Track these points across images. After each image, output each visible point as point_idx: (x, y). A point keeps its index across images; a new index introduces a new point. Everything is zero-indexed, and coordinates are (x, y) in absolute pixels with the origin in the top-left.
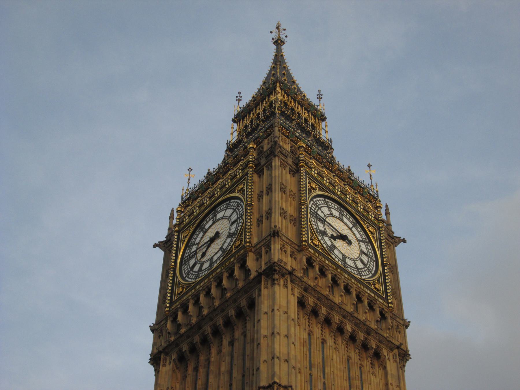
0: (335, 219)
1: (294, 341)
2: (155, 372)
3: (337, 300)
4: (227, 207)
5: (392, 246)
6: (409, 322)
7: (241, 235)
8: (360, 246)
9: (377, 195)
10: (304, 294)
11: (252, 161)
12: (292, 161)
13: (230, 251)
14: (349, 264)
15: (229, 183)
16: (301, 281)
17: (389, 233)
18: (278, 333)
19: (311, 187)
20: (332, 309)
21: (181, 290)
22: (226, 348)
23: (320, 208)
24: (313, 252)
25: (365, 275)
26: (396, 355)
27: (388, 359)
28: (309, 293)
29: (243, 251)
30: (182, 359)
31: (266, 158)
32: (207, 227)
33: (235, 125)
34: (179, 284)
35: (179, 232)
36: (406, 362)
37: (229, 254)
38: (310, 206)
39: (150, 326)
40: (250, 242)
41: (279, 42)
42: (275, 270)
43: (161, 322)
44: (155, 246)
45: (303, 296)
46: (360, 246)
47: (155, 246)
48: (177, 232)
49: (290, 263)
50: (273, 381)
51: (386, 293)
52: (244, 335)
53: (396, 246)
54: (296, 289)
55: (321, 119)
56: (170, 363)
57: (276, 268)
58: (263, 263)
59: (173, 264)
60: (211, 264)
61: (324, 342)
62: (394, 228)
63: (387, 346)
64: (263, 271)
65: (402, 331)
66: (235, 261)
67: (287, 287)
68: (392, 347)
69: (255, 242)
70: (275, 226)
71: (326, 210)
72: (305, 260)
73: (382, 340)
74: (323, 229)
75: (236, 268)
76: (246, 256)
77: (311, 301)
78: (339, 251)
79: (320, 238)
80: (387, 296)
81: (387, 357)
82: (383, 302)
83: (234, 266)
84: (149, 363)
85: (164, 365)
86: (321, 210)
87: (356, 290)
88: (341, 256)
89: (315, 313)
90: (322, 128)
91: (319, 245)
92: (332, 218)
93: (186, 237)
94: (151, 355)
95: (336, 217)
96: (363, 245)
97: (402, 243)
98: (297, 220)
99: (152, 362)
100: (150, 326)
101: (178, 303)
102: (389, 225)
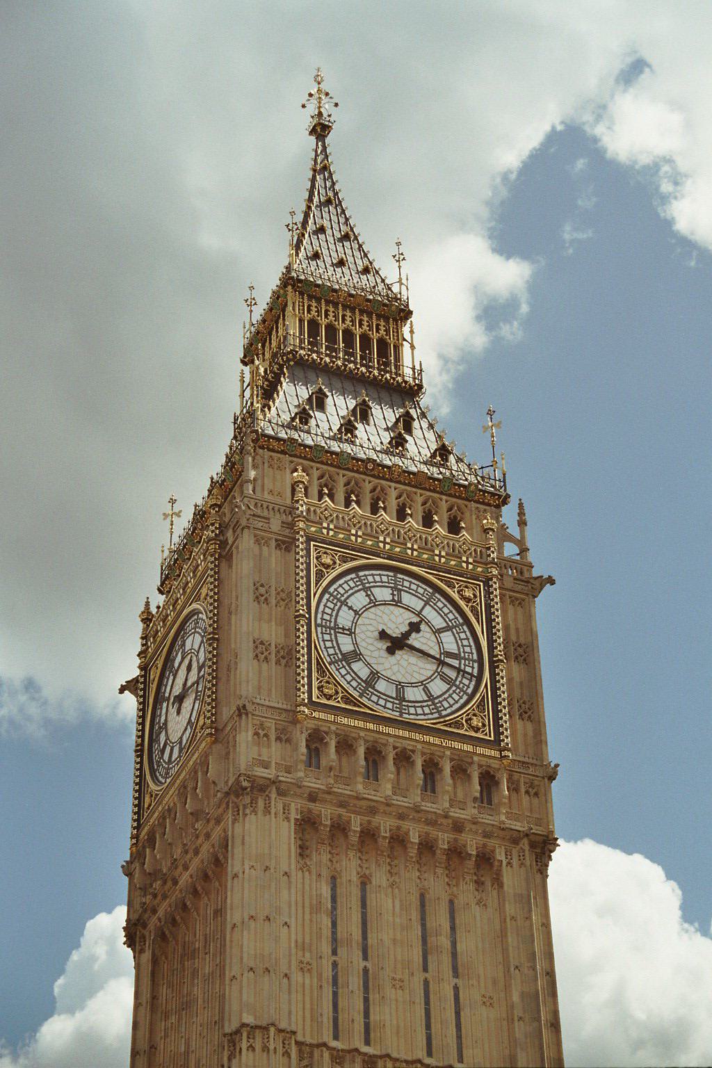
4: (195, 628)
6: (557, 766)
8: (440, 643)
10: (311, 805)
17: (522, 573)
19: (323, 565)
20: (373, 811)
23: (344, 603)
25: (451, 706)
26: (524, 851)
27: (509, 863)
32: (176, 665)
33: (247, 369)
36: (550, 858)
44: (122, 691)
45: (310, 811)
46: (440, 643)
47: (122, 691)
51: (497, 726)
57: (245, 784)
62: (531, 557)
67: (270, 813)
71: (359, 600)
77: (326, 813)
78: (388, 680)
80: (498, 734)
81: (504, 863)
84: (124, 944)
85: (142, 951)
86: (346, 605)
90: (405, 340)
91: (337, 693)
93: (154, 680)
95: (385, 604)
100: (123, 867)
101: (146, 829)
102: (524, 550)
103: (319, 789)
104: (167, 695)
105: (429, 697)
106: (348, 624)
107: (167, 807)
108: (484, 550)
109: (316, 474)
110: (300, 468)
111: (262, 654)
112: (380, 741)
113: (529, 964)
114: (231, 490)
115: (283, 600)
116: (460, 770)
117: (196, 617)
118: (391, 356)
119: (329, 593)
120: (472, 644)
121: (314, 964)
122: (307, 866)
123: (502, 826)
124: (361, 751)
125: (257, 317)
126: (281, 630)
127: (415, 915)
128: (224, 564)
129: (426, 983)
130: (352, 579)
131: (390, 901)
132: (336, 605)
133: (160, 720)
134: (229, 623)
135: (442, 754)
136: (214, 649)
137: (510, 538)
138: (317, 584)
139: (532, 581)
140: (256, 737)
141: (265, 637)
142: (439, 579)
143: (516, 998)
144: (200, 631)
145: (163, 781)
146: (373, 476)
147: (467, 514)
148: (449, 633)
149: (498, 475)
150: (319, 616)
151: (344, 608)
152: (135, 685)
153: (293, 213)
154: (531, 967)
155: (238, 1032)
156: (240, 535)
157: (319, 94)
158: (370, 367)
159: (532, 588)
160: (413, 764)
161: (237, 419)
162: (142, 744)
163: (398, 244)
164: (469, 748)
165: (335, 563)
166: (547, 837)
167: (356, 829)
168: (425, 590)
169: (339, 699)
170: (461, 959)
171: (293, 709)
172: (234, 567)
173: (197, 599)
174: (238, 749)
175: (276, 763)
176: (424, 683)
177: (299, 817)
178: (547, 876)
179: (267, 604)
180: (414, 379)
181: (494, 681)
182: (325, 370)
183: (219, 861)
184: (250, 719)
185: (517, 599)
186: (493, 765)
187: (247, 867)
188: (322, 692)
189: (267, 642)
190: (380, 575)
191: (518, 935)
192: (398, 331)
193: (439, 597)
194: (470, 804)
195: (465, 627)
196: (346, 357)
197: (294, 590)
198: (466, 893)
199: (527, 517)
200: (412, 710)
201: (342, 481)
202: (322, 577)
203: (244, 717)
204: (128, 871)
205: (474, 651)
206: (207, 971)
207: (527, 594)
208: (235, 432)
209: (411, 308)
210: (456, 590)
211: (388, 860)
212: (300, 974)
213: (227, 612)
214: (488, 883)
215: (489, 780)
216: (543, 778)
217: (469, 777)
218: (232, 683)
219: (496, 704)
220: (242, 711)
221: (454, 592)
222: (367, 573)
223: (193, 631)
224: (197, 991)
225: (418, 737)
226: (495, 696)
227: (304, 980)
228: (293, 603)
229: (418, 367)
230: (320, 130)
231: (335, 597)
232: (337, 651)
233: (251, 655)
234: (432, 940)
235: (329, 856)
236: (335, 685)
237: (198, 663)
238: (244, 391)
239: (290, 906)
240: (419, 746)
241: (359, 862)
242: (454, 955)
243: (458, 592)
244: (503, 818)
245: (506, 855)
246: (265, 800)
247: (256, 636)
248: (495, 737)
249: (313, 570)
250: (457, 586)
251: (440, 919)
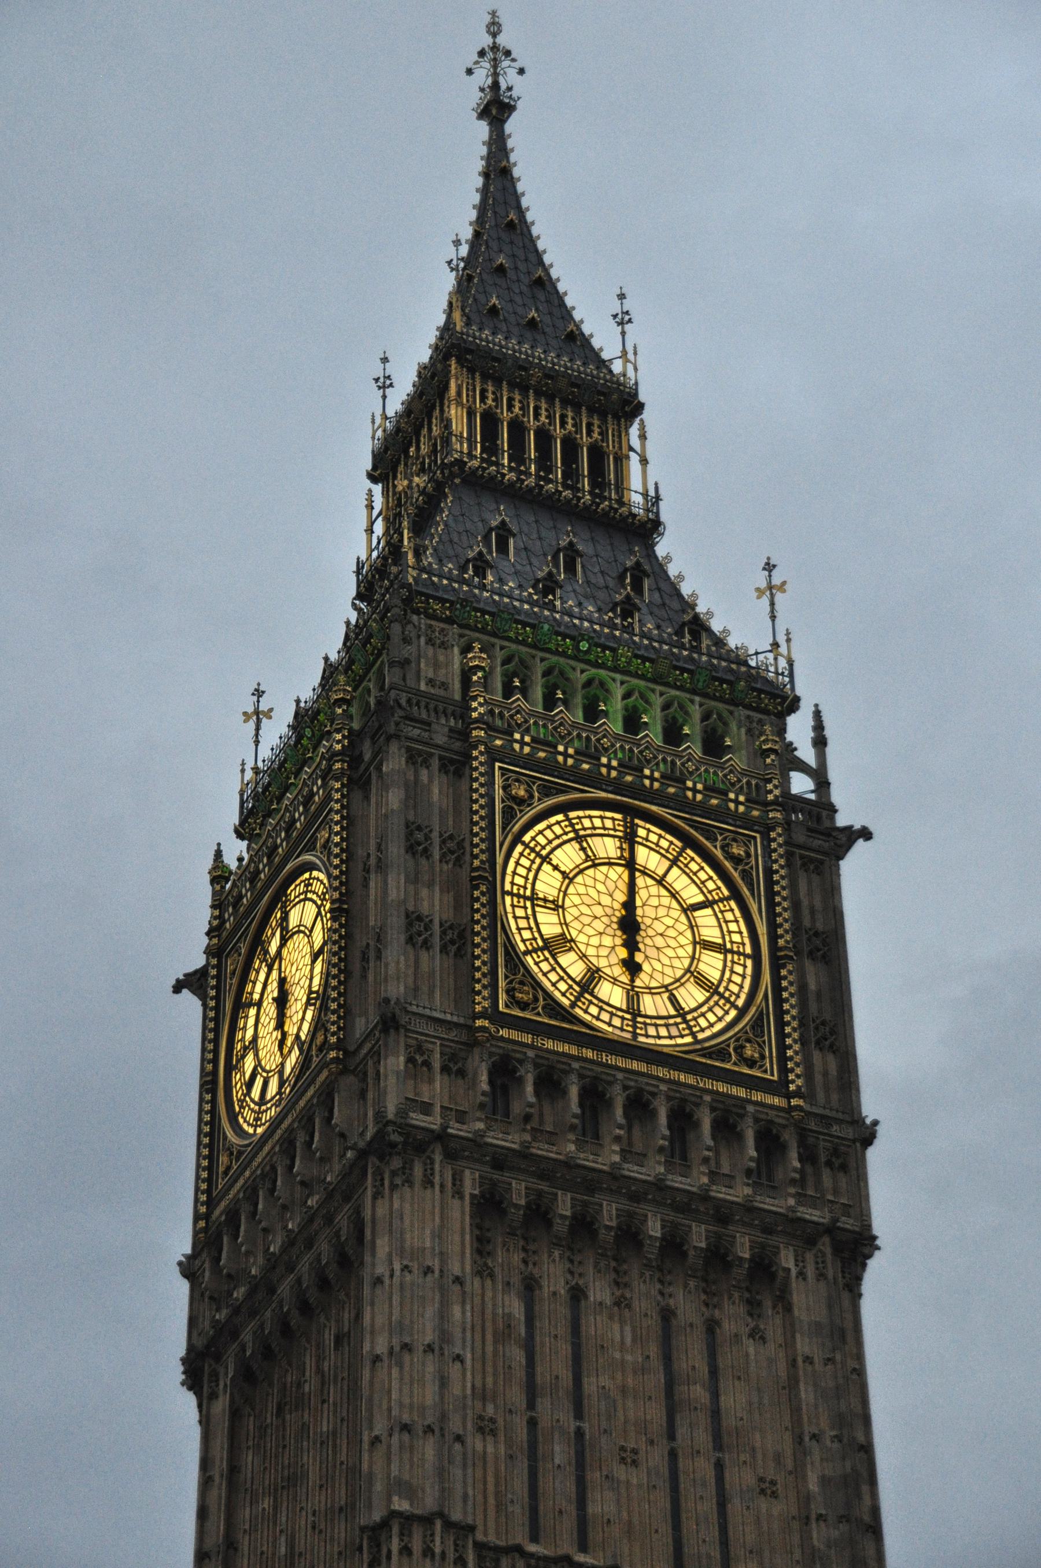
2: (200, 1411)
4: (306, 892)
6: (876, 1123)
10: (496, 1176)
14: (651, 1012)
17: (819, 819)
23: (546, 859)
25: (711, 1025)
26: (824, 1255)
27: (801, 1274)
30: (247, 1375)
31: (372, 738)
33: (377, 489)
34: (224, 1133)
36: (864, 1266)
37: (308, 1069)
39: (180, 1264)
42: (393, 1145)
47: (178, 988)
53: (842, 858)
56: (226, 1385)
57: (395, 1138)
60: (282, 1083)
66: (315, 1101)
69: (358, 1036)
70: (387, 1001)
71: (568, 856)
74: (558, 930)
75: (317, 1121)
77: (519, 1191)
80: (784, 1070)
81: (794, 1272)
85: (213, 1396)
86: (549, 863)
90: (631, 449)
91: (536, 999)
93: (234, 973)
94: (184, 1361)
97: (860, 842)
100: (180, 1264)
102: (822, 784)
103: (508, 1149)
104: (256, 997)
105: (676, 1010)
106: (552, 893)
107: (259, 1172)
109: (500, 656)
110: (477, 646)
111: (420, 936)
112: (604, 1077)
113: (833, 1433)
114: (362, 678)
115: (452, 852)
116: (727, 1126)
117: (307, 875)
118: (609, 475)
119: (523, 843)
120: (744, 929)
121: (501, 1422)
122: (488, 1268)
124: (574, 1092)
125: (395, 405)
126: (449, 898)
127: (654, 1349)
128: (357, 795)
129: (673, 1455)
130: (558, 823)
131: (616, 1327)
132: (533, 862)
133: (243, 1037)
134: (366, 885)
136: (341, 925)
137: (801, 766)
138: (504, 829)
139: (834, 834)
140: (410, 1065)
141: (425, 908)
142: (691, 826)
143: (813, 1485)
144: (314, 897)
145: (251, 1131)
146: (588, 662)
147: (734, 726)
148: (708, 911)
149: (783, 663)
150: (508, 879)
151: (546, 867)
152: (199, 979)
153: (457, 243)
154: (836, 1436)
155: (385, 1524)
156: (384, 748)
157: (495, 53)
158: (578, 490)
159: (835, 844)
160: (653, 1114)
161: (363, 567)
162: (215, 1072)
163: (622, 297)
164: (742, 1093)
165: (531, 796)
166: (860, 1234)
167: (564, 1213)
168: (671, 843)
169: (540, 1009)
170: (729, 1421)
171: (469, 1022)
172: (373, 800)
173: (310, 847)
174: (382, 1084)
175: (442, 1107)
176: (670, 988)
177: (476, 1192)
178: (860, 1295)
179: (428, 858)
180: (648, 510)
181: (777, 989)
182: (513, 494)
183: (349, 1259)
184: (402, 1040)
185: (812, 860)
187: (397, 1267)
188: (513, 997)
189: (427, 916)
190: (601, 817)
191: (815, 1385)
192: (621, 434)
193: (692, 854)
194: (740, 1178)
195: (733, 904)
196: (542, 473)
197: (467, 836)
198: (733, 1318)
199: (827, 733)
200: (652, 1031)
201: (539, 668)
202: (513, 818)
203: (392, 1031)
204: (189, 1269)
205: (747, 941)
206: (325, 1429)
208: (358, 586)
209: (642, 397)
210: (718, 844)
211: (613, 1264)
212: (479, 1436)
213: (361, 866)
214: (768, 1303)
215: (769, 1142)
217: (740, 1137)
218: (371, 977)
219: (781, 1024)
220: (390, 1023)
221: (715, 847)
222: (581, 813)
223: (302, 897)
224: (312, 1464)
225: (661, 1072)
226: (780, 1013)
227: (485, 1446)
228: (467, 857)
229: (652, 493)
230: (496, 109)
231: (533, 850)
232: (536, 935)
233: (403, 938)
234: (681, 1390)
235: (522, 1255)
236: (534, 988)
237: (312, 947)
238: (373, 523)
239: (464, 1330)
240: (663, 1087)
241: (568, 1265)
242: (716, 1413)
243: (722, 848)
244: (791, 1202)
245: (796, 1260)
246: (425, 1164)
247: (411, 909)
248: (779, 1077)
250: (720, 838)
251: (692, 1355)
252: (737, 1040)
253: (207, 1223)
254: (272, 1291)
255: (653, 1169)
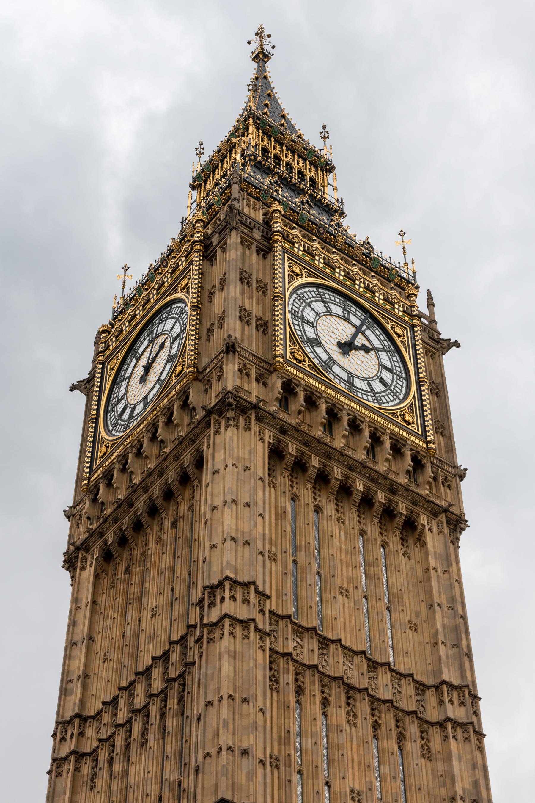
0: (336, 318)
1: (261, 512)
2: (72, 580)
3: (339, 443)
5: (437, 354)
6: (466, 470)
7: (183, 356)
9: (414, 277)
11: (200, 241)
12: (260, 234)
13: (169, 382)
15: (168, 281)
16: (275, 418)
18: (234, 501)
21: (103, 450)
22: (168, 533)
24: (294, 372)
25: (388, 402)
26: (442, 522)
27: (430, 529)
28: (289, 435)
29: (185, 380)
30: (107, 556)
31: (219, 233)
32: (140, 351)
33: (194, 193)
35: (103, 363)
36: (460, 533)
38: (291, 301)
39: (65, 511)
40: (194, 365)
41: (261, 57)
42: (230, 404)
43: (80, 502)
44: (73, 388)
45: (279, 441)
47: (73, 388)
48: (100, 364)
49: (254, 391)
50: (224, 576)
51: (424, 427)
52: (191, 508)
53: (443, 354)
54: (267, 431)
55: (326, 170)
56: (92, 563)
57: (232, 401)
58: (213, 395)
59: (95, 412)
61: (318, 510)
62: (440, 327)
63: (426, 510)
64: (213, 408)
65: (454, 485)
67: (250, 429)
68: (435, 512)
70: (230, 336)
71: (319, 307)
72: (280, 385)
73: (417, 501)
74: (314, 336)
76: (189, 389)
77: (293, 448)
78: (341, 367)
79: (308, 350)
80: (425, 431)
81: (427, 527)
82: (417, 441)
83: (173, 405)
84: (63, 567)
85: (83, 569)
86: (310, 306)
87: (370, 426)
88: (344, 376)
89: (300, 466)
90: (329, 184)
91: (304, 361)
92: (329, 317)
93: (113, 369)
94: (65, 554)
95: (338, 316)
96: (384, 356)
97: (454, 348)
98: (269, 324)
99: (67, 565)
100: (65, 511)
102: (433, 321)
106: (312, 320)
108: (409, 308)
112: (338, 405)
119: (297, 294)
120: (401, 366)
122: (273, 483)
123: (428, 498)
124: (323, 407)
135: (383, 431)
138: (289, 283)
139: (441, 342)
146: (322, 239)
151: (307, 307)
154: (450, 607)
155: (221, 584)
165: (302, 275)
177: (271, 441)
181: (420, 396)
186: (421, 452)
188: (294, 356)
203: (231, 353)
205: (403, 372)
207: (437, 350)
216: (455, 475)
222: (325, 292)
225: (366, 412)
243: (392, 328)
246: (246, 420)
249: (287, 273)
252: (401, 411)
253: (89, 482)
254: (131, 505)
255: (361, 456)
